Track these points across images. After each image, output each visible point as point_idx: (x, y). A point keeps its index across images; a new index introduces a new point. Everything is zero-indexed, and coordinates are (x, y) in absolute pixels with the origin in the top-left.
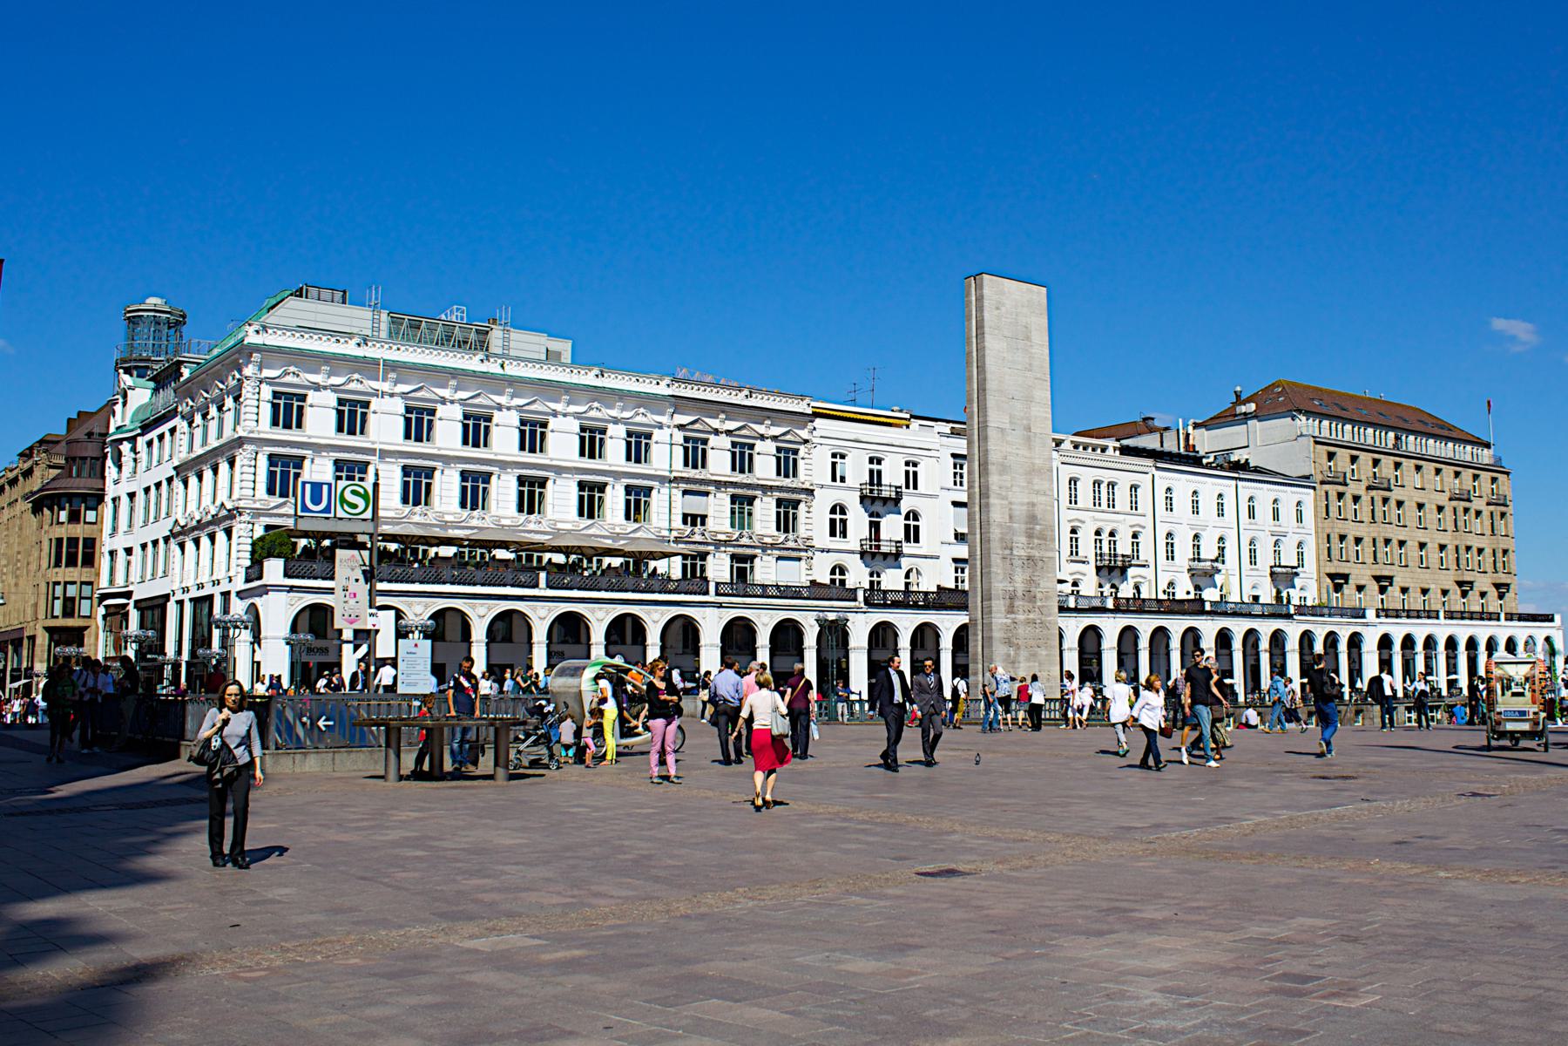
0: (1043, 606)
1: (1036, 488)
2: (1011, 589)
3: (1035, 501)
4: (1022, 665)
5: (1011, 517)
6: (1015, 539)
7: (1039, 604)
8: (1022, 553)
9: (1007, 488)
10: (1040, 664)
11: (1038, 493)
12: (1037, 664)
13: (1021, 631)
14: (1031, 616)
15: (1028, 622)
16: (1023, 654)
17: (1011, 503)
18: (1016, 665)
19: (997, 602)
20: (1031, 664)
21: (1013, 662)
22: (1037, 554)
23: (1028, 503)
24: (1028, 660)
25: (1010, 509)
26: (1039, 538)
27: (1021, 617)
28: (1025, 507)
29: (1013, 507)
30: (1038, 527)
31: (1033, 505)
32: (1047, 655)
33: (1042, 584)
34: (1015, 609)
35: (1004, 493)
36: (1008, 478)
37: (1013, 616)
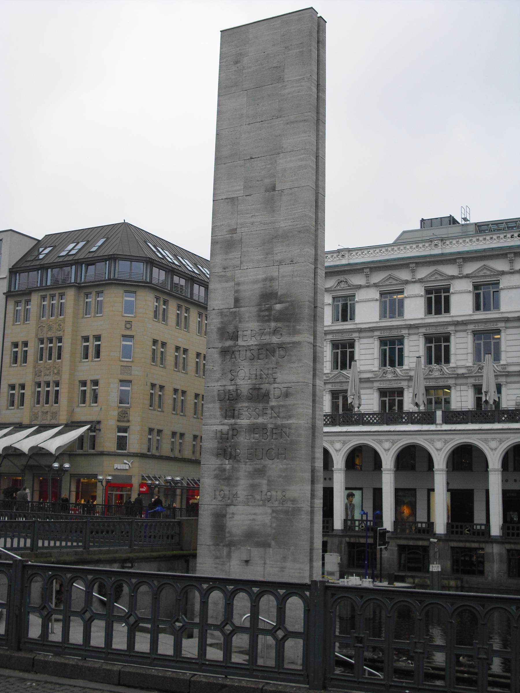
0: (279, 406)
1: (278, 257)
2: (231, 388)
3: (276, 274)
5: (237, 301)
6: (241, 326)
7: (273, 403)
8: (253, 342)
9: (235, 267)
11: (281, 263)
15: (253, 429)
17: (238, 284)
18: (233, 482)
19: (211, 405)
23: (265, 280)
25: (237, 291)
27: (244, 421)
28: (260, 285)
29: (241, 288)
30: (278, 307)
31: (272, 279)
33: (280, 377)
34: (236, 413)
35: (229, 274)
36: (237, 254)
37: (232, 421)
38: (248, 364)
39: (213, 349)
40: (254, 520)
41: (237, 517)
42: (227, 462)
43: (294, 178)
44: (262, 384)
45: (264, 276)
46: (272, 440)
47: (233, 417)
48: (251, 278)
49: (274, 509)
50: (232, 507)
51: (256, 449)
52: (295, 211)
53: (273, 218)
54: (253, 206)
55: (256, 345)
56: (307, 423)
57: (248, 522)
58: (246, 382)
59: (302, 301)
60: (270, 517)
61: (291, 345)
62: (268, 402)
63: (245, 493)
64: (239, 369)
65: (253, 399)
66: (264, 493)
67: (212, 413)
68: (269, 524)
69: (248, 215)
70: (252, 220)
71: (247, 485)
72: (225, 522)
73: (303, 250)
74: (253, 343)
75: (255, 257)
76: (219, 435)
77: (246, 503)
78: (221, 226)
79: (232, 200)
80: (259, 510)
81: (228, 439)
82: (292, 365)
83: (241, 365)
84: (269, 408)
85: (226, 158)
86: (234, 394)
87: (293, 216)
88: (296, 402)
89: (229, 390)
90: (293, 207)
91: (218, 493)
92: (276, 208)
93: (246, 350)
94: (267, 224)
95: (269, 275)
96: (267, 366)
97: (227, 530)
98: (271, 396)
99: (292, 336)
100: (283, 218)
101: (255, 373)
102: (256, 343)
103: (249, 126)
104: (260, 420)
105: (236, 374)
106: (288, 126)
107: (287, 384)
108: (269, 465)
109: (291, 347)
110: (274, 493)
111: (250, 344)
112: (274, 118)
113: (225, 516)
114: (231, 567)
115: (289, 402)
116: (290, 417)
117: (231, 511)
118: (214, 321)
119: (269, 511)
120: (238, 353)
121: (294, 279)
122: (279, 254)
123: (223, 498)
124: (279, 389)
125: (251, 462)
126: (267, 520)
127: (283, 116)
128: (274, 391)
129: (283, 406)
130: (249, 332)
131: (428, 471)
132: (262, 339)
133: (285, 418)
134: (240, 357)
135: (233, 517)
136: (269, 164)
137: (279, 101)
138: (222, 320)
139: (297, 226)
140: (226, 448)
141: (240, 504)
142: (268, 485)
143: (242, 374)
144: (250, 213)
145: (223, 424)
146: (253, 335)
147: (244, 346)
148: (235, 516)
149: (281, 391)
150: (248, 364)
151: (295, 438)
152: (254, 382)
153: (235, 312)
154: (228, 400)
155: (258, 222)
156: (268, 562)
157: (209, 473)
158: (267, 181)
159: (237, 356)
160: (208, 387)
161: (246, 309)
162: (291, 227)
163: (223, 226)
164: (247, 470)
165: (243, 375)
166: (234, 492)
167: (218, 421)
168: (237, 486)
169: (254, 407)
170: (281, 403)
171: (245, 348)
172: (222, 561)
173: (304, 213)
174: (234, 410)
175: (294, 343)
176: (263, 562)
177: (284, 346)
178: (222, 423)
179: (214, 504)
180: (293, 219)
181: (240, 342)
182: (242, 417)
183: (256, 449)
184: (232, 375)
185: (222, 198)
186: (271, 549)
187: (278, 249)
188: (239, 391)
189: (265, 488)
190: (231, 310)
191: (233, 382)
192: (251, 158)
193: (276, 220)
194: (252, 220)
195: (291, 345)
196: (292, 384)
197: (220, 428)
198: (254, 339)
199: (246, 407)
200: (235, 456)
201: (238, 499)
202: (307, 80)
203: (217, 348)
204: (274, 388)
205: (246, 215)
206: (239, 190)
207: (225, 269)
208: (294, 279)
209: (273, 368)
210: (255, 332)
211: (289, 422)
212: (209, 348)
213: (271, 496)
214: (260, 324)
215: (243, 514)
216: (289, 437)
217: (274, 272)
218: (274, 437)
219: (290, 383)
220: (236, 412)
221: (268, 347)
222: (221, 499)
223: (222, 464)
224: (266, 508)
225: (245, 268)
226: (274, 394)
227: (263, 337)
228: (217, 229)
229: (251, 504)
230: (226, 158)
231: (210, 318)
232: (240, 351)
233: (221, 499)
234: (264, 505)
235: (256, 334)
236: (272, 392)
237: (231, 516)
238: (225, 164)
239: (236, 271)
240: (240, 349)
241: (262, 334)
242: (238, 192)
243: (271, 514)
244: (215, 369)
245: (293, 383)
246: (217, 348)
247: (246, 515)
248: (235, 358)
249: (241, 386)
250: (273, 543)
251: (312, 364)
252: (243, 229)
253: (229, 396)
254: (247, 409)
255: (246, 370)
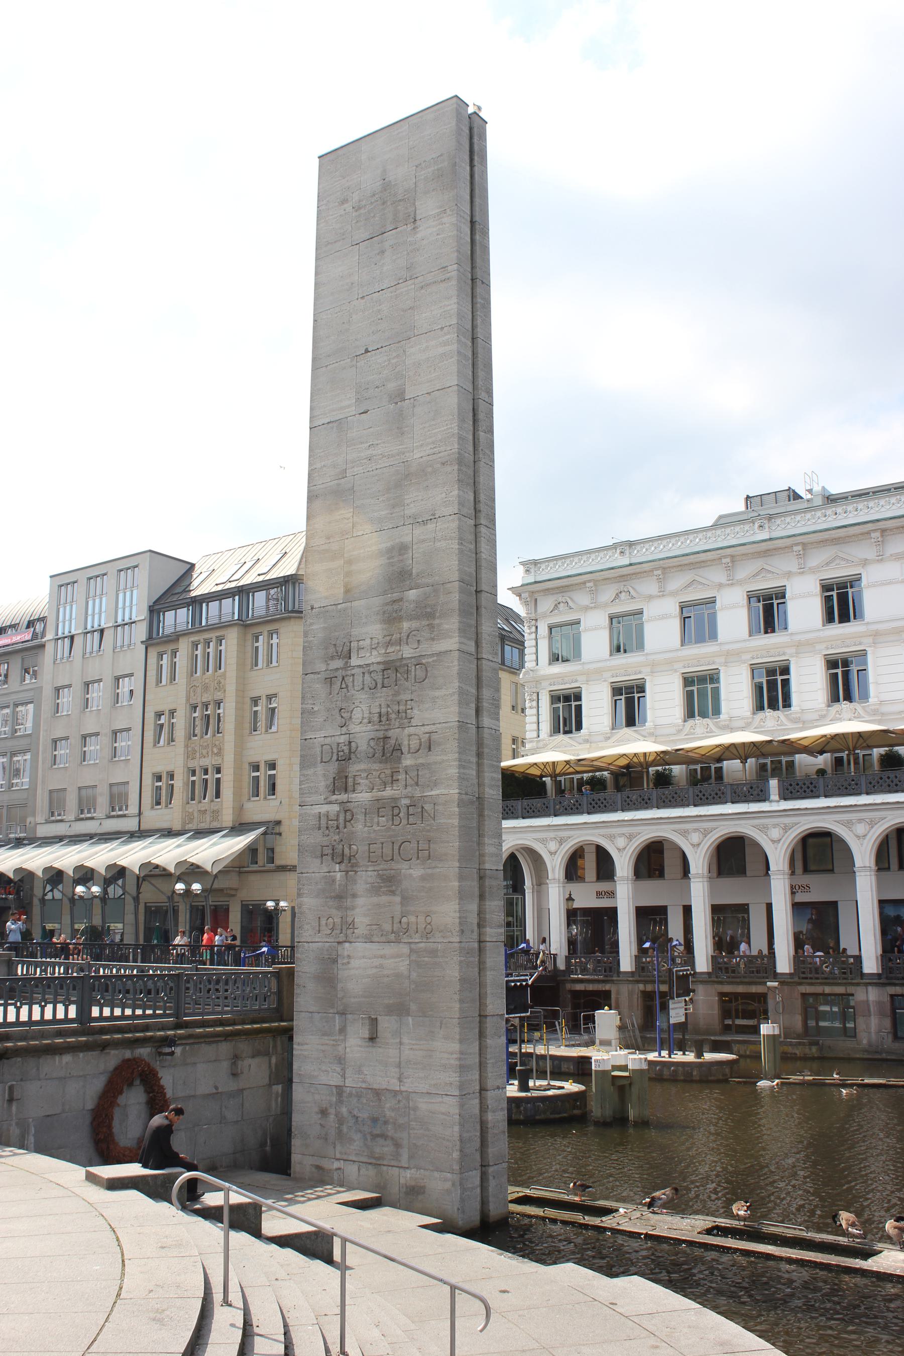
0: (417, 768)
4: (360, 901)
6: (355, 632)
7: (408, 761)
10: (405, 900)
12: (398, 899)
13: (359, 827)
14: (389, 792)
16: (365, 877)
17: (350, 562)
18: (349, 902)
20: (384, 899)
21: (340, 897)
22: (407, 652)
23: (390, 550)
24: (375, 890)
25: (348, 574)
26: (411, 618)
27: (362, 797)
30: (412, 594)
31: (402, 549)
32: (423, 878)
37: (343, 797)
38: (367, 696)
39: (312, 676)
40: (381, 966)
41: (355, 963)
42: (337, 867)
43: (433, 375)
44: (390, 729)
45: (389, 545)
46: (408, 826)
47: (346, 790)
48: (369, 549)
49: (413, 946)
50: (347, 945)
51: (382, 843)
52: (436, 430)
53: (401, 445)
54: (371, 429)
55: (378, 663)
56: (466, 794)
57: (374, 971)
58: (365, 728)
59: (450, 580)
60: (408, 962)
61: (435, 658)
62: (399, 760)
63: (366, 920)
64: (354, 706)
65: (376, 755)
66: (396, 920)
67: (312, 785)
68: (406, 973)
69: (363, 445)
70: (369, 452)
71: (370, 907)
72: (335, 971)
73: (452, 494)
74: (374, 660)
75: (375, 514)
76: (323, 822)
77: (369, 939)
78: (322, 468)
79: (339, 424)
80: (389, 950)
81: (338, 828)
82: (437, 693)
83: (356, 699)
84: (401, 770)
85: (329, 356)
86: (346, 749)
87: (434, 439)
88: (445, 758)
89: (338, 744)
90: (433, 423)
91: (323, 922)
92: (406, 429)
93: (364, 673)
94: (393, 456)
95: (397, 541)
96: (398, 698)
97: (340, 985)
98: (405, 749)
99: (435, 642)
100: (417, 444)
101: (378, 710)
102: (379, 660)
103: (363, 301)
104: (389, 792)
105: (349, 714)
106: (423, 291)
107: (430, 726)
108: (403, 871)
109: (433, 661)
110: (412, 919)
111: (370, 662)
112: (401, 281)
113: (335, 961)
114: (348, 1050)
115: (433, 758)
116: (436, 784)
117: (346, 953)
118: (314, 627)
119: (405, 949)
120: (351, 680)
121: (438, 544)
122: (412, 505)
123: (332, 929)
124: (416, 737)
125: (374, 866)
126: (403, 966)
127: (415, 276)
128: (409, 741)
129: (423, 765)
130: (368, 641)
131: (596, 882)
132: (388, 651)
133: (428, 786)
134: (353, 686)
135: (348, 963)
136: (394, 358)
137: (408, 254)
138: (326, 625)
139: (439, 455)
140: (335, 843)
141: (359, 940)
142: (402, 903)
143: (357, 715)
144: (367, 442)
145: (330, 803)
146: (373, 647)
147: (360, 666)
148: (352, 961)
149: (420, 739)
150: (367, 696)
151: (445, 821)
152: (377, 727)
153: (345, 610)
154: (338, 760)
155: (379, 455)
156: (405, 1040)
157: (310, 887)
158: (391, 386)
159: (350, 684)
160: (306, 739)
161: (362, 602)
162: (430, 458)
163: (325, 468)
164: (369, 880)
165: (360, 716)
166: (350, 920)
167: (323, 797)
168: (353, 908)
169: (378, 771)
170: (421, 761)
171: (362, 670)
172: (334, 1040)
173: (450, 430)
174: (346, 777)
175: (439, 654)
176: (398, 1040)
177: (424, 661)
178: (329, 800)
179: (319, 940)
180: (433, 443)
181: (354, 661)
182: (359, 788)
183: (382, 843)
184: (342, 717)
185: (323, 422)
186: (410, 1019)
187: (411, 496)
188: (353, 744)
189: (398, 908)
190: (339, 607)
191: (344, 729)
192: (367, 351)
193: (406, 448)
194: (369, 452)
195: (435, 658)
196: (438, 726)
197: (324, 809)
198: (375, 653)
199: (365, 770)
200: (350, 856)
201: (355, 931)
202: (451, 213)
203: (318, 673)
204: (410, 736)
205: (360, 446)
206: (349, 406)
207: (328, 538)
208: (438, 544)
209: (406, 701)
210: (376, 641)
211: (433, 793)
212: (306, 674)
213: (408, 924)
214: (385, 626)
215: (364, 957)
216: (434, 820)
217: (406, 535)
218: (411, 819)
219: (434, 724)
220: (350, 780)
221: (398, 664)
222: (329, 932)
223: (329, 872)
224: (401, 945)
225: (360, 533)
226: (409, 745)
227: (390, 650)
228: (316, 474)
229: (376, 939)
230: (329, 356)
231: (308, 623)
232: (353, 675)
233: (329, 932)
234: (398, 941)
235: (378, 643)
236: (406, 743)
237: (345, 961)
238: (326, 366)
239: (346, 541)
240: (353, 672)
241: (389, 644)
242: (347, 410)
243: (409, 956)
244: (316, 709)
245: (440, 723)
246: (318, 673)
247: (370, 959)
248: (347, 686)
249: (357, 735)
250: (413, 1007)
251: (473, 691)
252: (356, 469)
253: (338, 754)
254: (366, 775)
255: (364, 707)
